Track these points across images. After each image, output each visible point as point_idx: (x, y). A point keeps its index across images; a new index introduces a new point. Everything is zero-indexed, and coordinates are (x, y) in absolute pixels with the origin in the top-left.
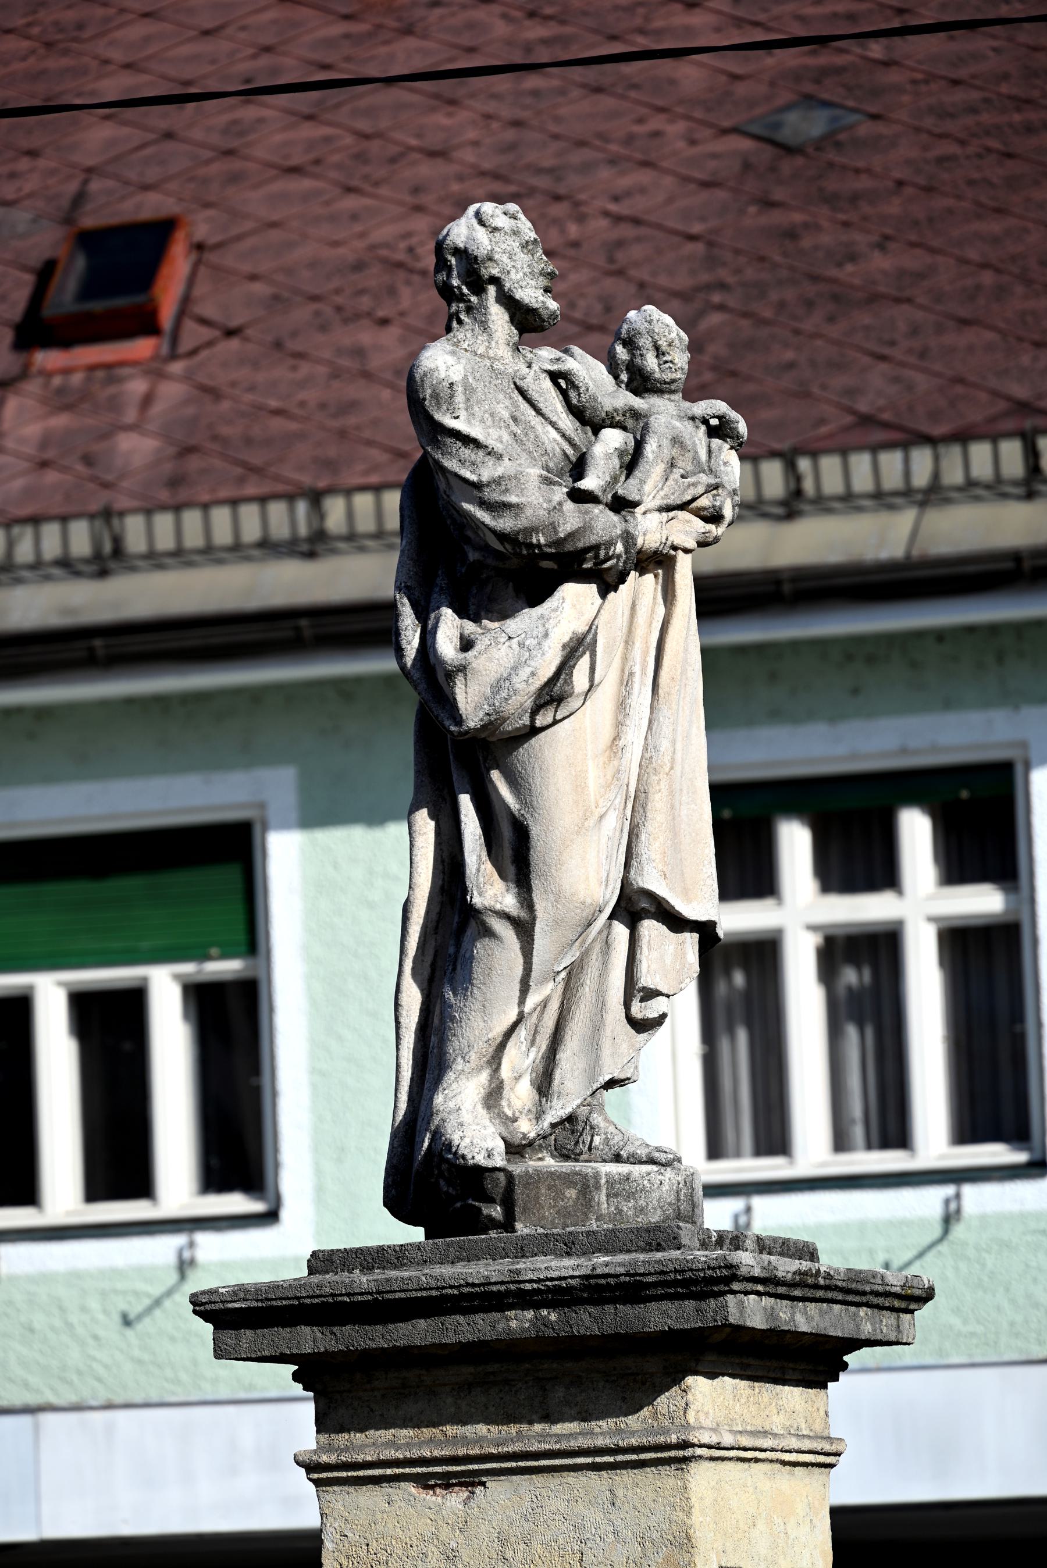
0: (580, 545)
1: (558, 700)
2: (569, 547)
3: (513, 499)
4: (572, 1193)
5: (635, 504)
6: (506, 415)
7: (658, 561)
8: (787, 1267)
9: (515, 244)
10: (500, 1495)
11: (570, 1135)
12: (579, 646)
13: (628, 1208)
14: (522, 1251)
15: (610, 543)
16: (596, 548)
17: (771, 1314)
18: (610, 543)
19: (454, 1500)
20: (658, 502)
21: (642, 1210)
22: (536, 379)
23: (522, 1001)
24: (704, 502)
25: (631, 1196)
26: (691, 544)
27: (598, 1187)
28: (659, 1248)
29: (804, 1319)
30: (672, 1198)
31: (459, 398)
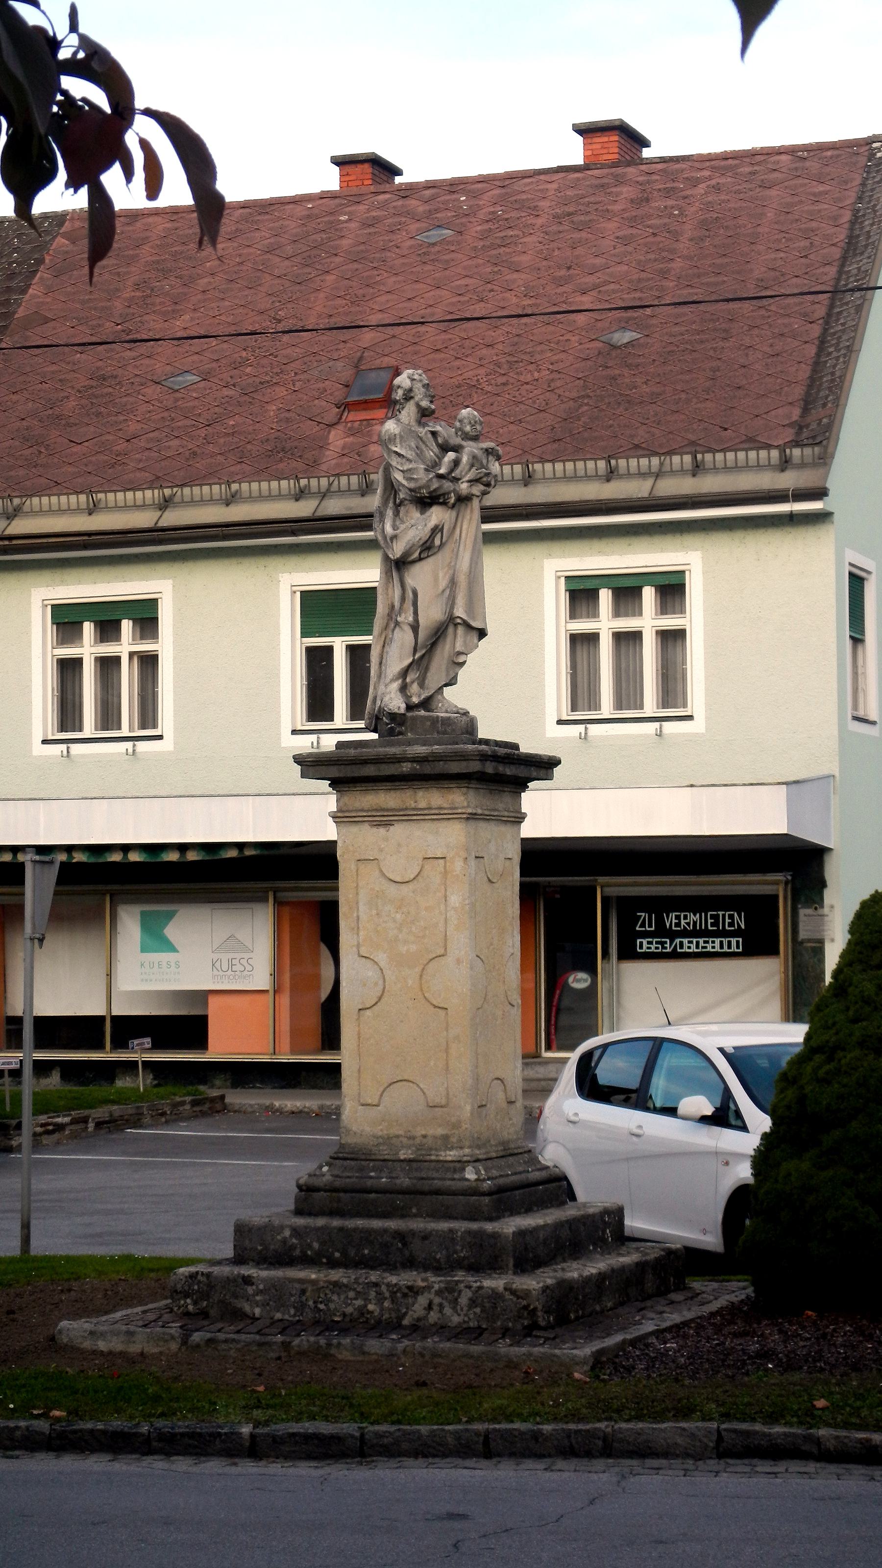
0: (438, 493)
1: (429, 548)
2: (434, 494)
3: (415, 477)
4: (429, 723)
5: (459, 479)
6: (414, 446)
8: (502, 751)
9: (420, 385)
10: (399, 831)
11: (426, 704)
12: (437, 530)
13: (449, 730)
14: (409, 743)
15: (449, 493)
16: (444, 494)
17: (496, 768)
18: (449, 493)
19: (382, 830)
20: (467, 478)
22: (426, 433)
23: (414, 654)
24: (485, 479)
25: (450, 725)
26: (478, 494)
27: (438, 721)
28: (457, 744)
29: (509, 771)
31: (398, 440)
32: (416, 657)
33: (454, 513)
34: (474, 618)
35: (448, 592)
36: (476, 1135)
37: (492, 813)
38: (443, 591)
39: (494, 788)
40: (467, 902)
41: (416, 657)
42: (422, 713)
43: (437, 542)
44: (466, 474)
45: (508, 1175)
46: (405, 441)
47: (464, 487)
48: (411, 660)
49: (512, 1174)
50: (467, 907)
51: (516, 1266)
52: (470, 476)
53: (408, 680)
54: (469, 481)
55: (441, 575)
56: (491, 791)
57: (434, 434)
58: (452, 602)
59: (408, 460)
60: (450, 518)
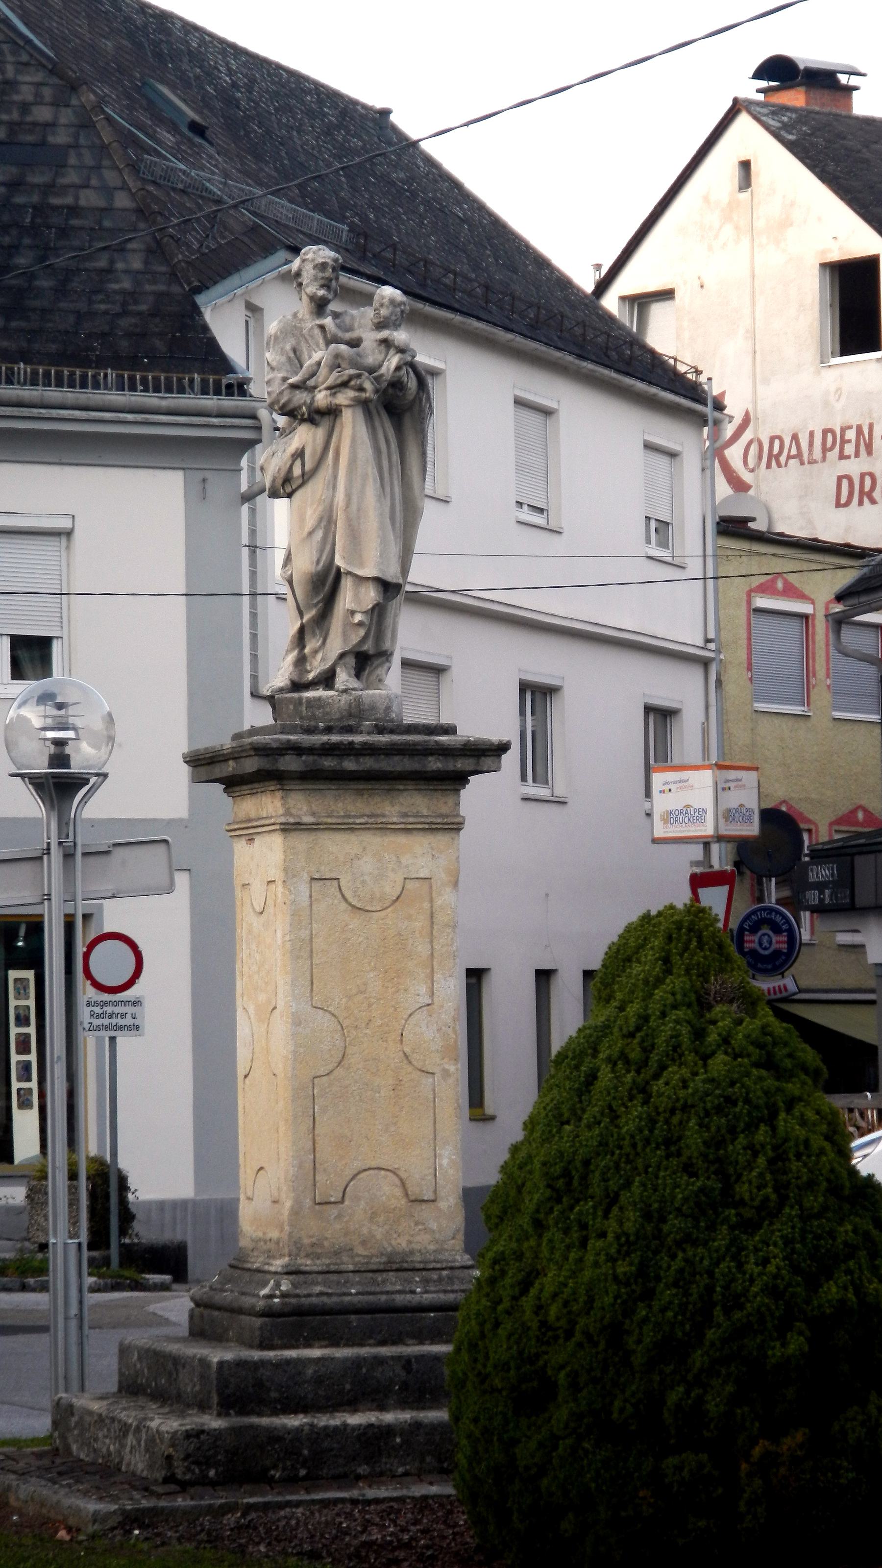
4: (291, 707)
6: (288, 347)
7: (332, 413)
12: (299, 454)
15: (300, 407)
18: (300, 407)
21: (328, 713)
22: (312, 328)
23: (302, 617)
32: (305, 620)
33: (320, 433)
34: (361, 565)
35: (319, 534)
36: (306, 1241)
37: (346, 821)
38: (310, 534)
39: (361, 787)
40: (288, 938)
41: (305, 620)
42: (319, 693)
43: (297, 471)
45: (351, 1294)
47: (322, 398)
48: (297, 625)
49: (357, 1294)
50: (288, 945)
51: (221, 1404)
52: (330, 382)
53: (307, 650)
54: (328, 388)
55: (309, 512)
56: (360, 793)
57: (322, 328)
58: (328, 544)
59: (272, 369)
60: (314, 440)
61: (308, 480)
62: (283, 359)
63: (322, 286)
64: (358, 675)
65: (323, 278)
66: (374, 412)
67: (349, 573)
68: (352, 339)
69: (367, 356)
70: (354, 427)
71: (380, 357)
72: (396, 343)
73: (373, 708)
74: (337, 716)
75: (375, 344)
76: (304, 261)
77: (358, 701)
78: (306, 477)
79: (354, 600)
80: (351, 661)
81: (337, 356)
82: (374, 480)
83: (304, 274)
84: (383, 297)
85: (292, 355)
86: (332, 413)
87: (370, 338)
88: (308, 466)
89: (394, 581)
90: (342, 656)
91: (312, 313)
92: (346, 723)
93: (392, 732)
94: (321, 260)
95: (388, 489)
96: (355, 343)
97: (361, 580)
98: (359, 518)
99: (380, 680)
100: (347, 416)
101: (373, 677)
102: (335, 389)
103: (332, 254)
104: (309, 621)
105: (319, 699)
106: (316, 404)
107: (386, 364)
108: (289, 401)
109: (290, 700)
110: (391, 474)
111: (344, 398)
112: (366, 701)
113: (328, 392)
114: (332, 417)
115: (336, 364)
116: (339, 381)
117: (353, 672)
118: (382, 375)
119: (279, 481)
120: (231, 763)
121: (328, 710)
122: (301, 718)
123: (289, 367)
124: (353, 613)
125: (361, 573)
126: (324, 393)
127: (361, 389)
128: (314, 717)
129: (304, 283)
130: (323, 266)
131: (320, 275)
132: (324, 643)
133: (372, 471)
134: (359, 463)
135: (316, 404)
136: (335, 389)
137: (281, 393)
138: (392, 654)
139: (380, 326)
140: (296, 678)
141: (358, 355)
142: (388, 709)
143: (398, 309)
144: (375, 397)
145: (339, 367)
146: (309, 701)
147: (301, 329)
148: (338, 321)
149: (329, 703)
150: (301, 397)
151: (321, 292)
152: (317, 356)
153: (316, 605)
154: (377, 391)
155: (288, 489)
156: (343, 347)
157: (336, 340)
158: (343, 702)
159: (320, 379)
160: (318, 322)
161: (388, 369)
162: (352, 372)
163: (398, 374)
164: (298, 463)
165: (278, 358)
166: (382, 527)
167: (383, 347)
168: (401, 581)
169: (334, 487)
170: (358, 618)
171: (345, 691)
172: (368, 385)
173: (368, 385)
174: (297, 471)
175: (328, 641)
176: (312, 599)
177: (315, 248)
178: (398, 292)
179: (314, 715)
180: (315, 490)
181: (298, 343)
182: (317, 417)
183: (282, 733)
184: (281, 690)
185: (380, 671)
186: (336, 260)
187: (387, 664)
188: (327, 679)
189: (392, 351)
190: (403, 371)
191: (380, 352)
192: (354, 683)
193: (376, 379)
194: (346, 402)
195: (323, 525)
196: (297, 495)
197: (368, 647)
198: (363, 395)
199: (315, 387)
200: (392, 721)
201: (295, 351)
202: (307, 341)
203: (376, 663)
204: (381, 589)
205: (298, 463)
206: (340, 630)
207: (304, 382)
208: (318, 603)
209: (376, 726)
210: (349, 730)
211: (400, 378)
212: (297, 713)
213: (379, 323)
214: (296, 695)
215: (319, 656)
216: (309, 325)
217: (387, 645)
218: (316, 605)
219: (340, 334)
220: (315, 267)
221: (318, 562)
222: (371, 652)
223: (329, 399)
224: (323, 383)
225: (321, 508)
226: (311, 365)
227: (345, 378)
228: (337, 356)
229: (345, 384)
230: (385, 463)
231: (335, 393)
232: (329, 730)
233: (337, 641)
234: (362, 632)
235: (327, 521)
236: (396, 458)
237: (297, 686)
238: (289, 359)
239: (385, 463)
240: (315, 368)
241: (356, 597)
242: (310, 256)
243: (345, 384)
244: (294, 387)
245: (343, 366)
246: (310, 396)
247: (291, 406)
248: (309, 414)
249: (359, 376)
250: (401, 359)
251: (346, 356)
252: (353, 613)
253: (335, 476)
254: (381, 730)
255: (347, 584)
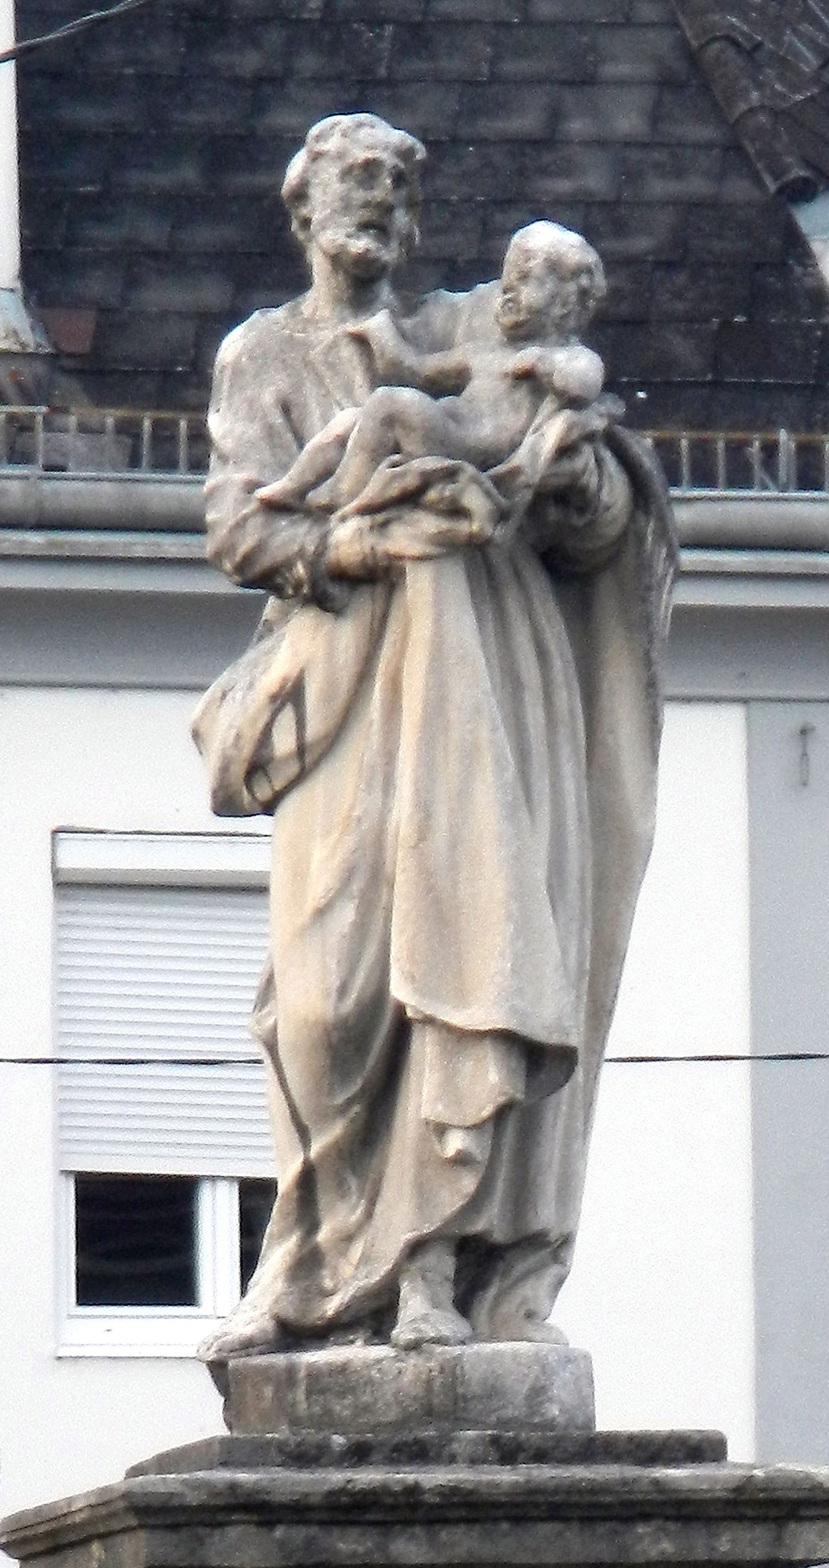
4: (268, 1391)
6: (268, 398)
9: (330, 172)
12: (291, 695)
13: (342, 1408)
15: (288, 564)
18: (288, 564)
20: (355, 504)
21: (366, 1408)
22: (333, 345)
25: (342, 1395)
30: (419, 1391)
33: (347, 634)
34: (461, 998)
35: (346, 915)
38: (322, 913)
43: (284, 742)
44: (363, 483)
46: (242, 389)
47: (348, 539)
52: (369, 493)
53: (323, 1236)
57: (361, 341)
60: (330, 656)
61: (317, 764)
62: (254, 430)
63: (364, 227)
64: (464, 1305)
65: (366, 205)
66: (505, 572)
67: (429, 1021)
68: (443, 374)
69: (478, 418)
70: (438, 620)
71: (512, 421)
72: (558, 381)
73: (493, 1391)
74: (392, 1415)
75: (503, 386)
76: (316, 157)
77: (452, 1372)
78: (309, 760)
79: (446, 1095)
80: (443, 1263)
81: (391, 421)
82: (498, 761)
83: (316, 194)
84: (528, 255)
85: (278, 420)
86: (377, 578)
87: (491, 364)
88: (315, 728)
89: (554, 1039)
90: (416, 1248)
91: (337, 300)
92: (407, 1436)
93: (540, 1457)
94: (361, 155)
95: (542, 786)
96: (447, 385)
97: (462, 1038)
98: (454, 867)
99: (530, 1315)
100: (419, 586)
101: (509, 1307)
102: (384, 510)
103: (398, 137)
104: (324, 1155)
105: (343, 1369)
106: (332, 555)
107: (529, 440)
108: (259, 549)
109: (265, 1373)
110: (552, 747)
111: (409, 536)
112: (474, 1374)
113: (366, 521)
114: (380, 590)
115: (388, 440)
116: (394, 491)
117: (447, 1293)
118: (515, 472)
119: (238, 770)
120: (96, 1548)
121: (366, 1398)
122: (295, 1422)
123: (267, 455)
124: (441, 1130)
125: (459, 1019)
126: (354, 523)
127: (456, 511)
128: (327, 1421)
129: (316, 217)
130: (369, 170)
131: (360, 195)
132: (369, 1215)
133: (490, 735)
134: (453, 715)
135: (332, 555)
136: (384, 510)
137: (240, 525)
138: (567, 1241)
139: (520, 334)
140: (290, 1312)
141: (453, 416)
142: (538, 1393)
143: (571, 287)
144: (500, 533)
145: (397, 450)
146: (315, 1375)
147: (306, 346)
148: (408, 323)
149: (370, 1382)
150: (292, 537)
151: (361, 244)
152: (343, 419)
153: (343, 1110)
154: (501, 516)
155: (264, 792)
156: (408, 396)
157: (396, 376)
158: (407, 1378)
159: (345, 486)
160: (353, 326)
161: (534, 453)
162: (432, 463)
163: (567, 466)
164: (287, 717)
165: (239, 428)
166: (519, 891)
167: (522, 395)
168: (575, 1040)
169: (388, 785)
170: (455, 1143)
171: (414, 1346)
172: (475, 500)
173: (475, 500)
174: (284, 742)
175: (379, 1208)
176: (331, 1092)
177: (346, 120)
178: (574, 239)
179: (328, 1412)
180: (336, 789)
181: (297, 387)
182: (335, 590)
183: (225, 1464)
184: (247, 1346)
185: (533, 1290)
186: (406, 154)
187: (554, 1271)
188: (375, 1315)
189: (548, 405)
190: (586, 457)
191: (516, 408)
192: (448, 1324)
193: (499, 481)
194: (416, 549)
195: (356, 887)
196: (289, 807)
197: (491, 1222)
198: (464, 528)
199: (329, 509)
200: (549, 1425)
201: (286, 408)
202: (320, 381)
203: (520, 1267)
204: (517, 1063)
205: (287, 717)
206: (409, 1177)
207: (302, 492)
208: (350, 1102)
209: (495, 1441)
210: (419, 1453)
211: (576, 477)
212: (283, 1409)
213: (517, 326)
214: (280, 1359)
215: (357, 1250)
216: (327, 335)
217: (545, 1217)
218: (343, 1110)
219: (411, 359)
220: (346, 173)
221: (343, 991)
222: (499, 1236)
223: (370, 541)
224: (353, 495)
225: (350, 842)
226: (322, 448)
227: (411, 482)
228: (391, 421)
229: (411, 499)
230: (535, 716)
231: (385, 525)
232: (359, 1454)
233: (401, 1210)
234: (469, 1183)
235: (367, 878)
236: (568, 698)
237: (291, 1334)
238: (270, 432)
239: (535, 716)
240: (332, 453)
241: (449, 1086)
242: (331, 145)
243: (411, 499)
244: (275, 508)
245: (408, 445)
246: (316, 532)
247: (265, 562)
248: (314, 585)
249: (450, 475)
250: (570, 428)
251: (415, 420)
252: (441, 1130)
253: (390, 755)
254: (508, 1454)
255: (424, 1049)
